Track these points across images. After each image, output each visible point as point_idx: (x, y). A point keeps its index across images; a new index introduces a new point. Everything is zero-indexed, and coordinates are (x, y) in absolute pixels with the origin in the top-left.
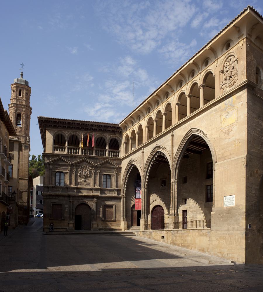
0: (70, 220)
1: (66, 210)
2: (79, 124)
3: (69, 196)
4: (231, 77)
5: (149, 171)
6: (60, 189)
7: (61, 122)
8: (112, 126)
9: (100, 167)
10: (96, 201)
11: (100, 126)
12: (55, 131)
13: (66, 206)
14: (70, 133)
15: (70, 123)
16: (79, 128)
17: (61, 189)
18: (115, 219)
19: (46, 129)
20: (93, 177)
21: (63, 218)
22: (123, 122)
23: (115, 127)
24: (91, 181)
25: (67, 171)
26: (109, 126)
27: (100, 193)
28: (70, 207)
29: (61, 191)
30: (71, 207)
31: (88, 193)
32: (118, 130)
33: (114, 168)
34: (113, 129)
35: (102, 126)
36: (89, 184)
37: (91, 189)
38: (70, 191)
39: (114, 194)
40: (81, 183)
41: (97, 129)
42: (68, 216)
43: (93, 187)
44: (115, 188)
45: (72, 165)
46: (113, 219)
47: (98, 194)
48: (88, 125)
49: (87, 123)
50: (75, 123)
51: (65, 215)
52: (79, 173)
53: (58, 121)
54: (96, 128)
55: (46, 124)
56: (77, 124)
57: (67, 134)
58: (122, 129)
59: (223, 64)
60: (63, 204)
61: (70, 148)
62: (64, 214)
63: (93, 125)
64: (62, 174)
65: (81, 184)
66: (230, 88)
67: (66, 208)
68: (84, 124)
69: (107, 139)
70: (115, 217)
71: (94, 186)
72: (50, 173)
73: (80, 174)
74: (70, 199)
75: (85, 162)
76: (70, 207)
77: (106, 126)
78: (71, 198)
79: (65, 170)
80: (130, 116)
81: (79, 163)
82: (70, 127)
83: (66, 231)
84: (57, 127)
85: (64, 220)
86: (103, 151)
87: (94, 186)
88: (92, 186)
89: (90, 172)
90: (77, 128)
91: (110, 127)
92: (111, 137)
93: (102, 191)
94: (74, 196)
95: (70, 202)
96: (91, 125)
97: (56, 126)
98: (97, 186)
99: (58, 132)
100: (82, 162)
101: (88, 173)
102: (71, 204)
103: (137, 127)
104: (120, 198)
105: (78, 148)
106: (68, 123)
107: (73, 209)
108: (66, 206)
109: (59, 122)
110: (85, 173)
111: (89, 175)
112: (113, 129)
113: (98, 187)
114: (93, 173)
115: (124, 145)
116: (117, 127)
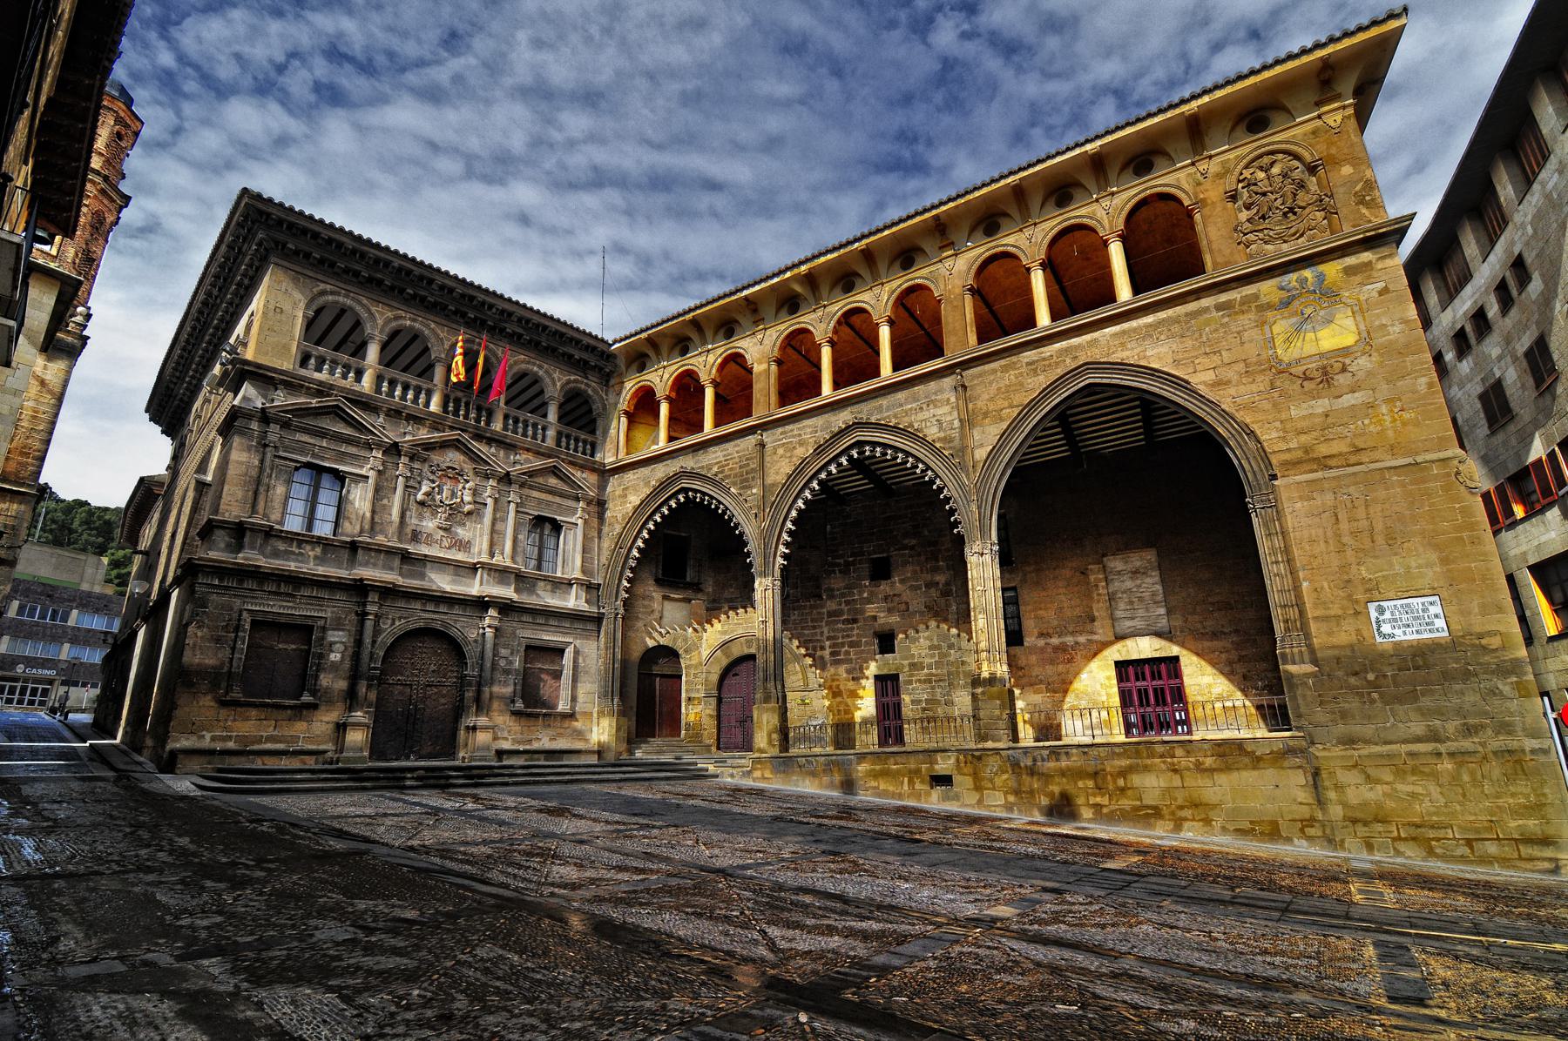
0: (351, 709)
1: (335, 657)
2: (451, 290)
3: (360, 589)
4: (1291, 210)
5: (794, 513)
6: (308, 547)
7: (363, 255)
8: (586, 340)
9: (522, 485)
10: (496, 623)
11: (538, 325)
12: (322, 286)
13: (335, 636)
14: (397, 318)
15: (409, 272)
16: (445, 308)
17: (318, 550)
18: (573, 708)
19: (273, 259)
20: (488, 519)
21: (306, 698)
22: (644, 335)
23: (594, 349)
24: (477, 536)
25: (363, 472)
26: (572, 339)
27: (516, 591)
28: (359, 642)
29: (316, 557)
30: (367, 640)
31: (453, 582)
32: (601, 363)
33: (577, 499)
34: (585, 356)
35: (545, 328)
36: (465, 546)
37: (474, 568)
38: (366, 564)
39: (574, 601)
40: (429, 535)
41: (520, 336)
42: (342, 685)
43: (485, 558)
44: (577, 574)
45: (393, 450)
46: (562, 706)
47: (508, 592)
48: (491, 306)
49: (489, 300)
50: (431, 281)
51: (325, 680)
52: (425, 489)
53: (350, 244)
54: (520, 330)
55: (281, 237)
56: (442, 287)
57: (379, 319)
58: (621, 362)
59: (1236, 173)
60: (321, 623)
61: (387, 376)
62: (317, 677)
63: (510, 314)
64: (326, 481)
65: (430, 540)
66: (1285, 247)
67: (332, 644)
68: (472, 298)
69: (554, 384)
70: (574, 699)
71: (492, 555)
72: (262, 461)
73: (427, 494)
74: (364, 605)
75: (458, 449)
76: (359, 642)
77: (562, 335)
78: (373, 597)
79: (345, 464)
80: (687, 317)
81: (429, 447)
82: (402, 291)
83: (319, 767)
84: (335, 273)
85: (314, 707)
86: (535, 426)
87: (492, 555)
88: (480, 553)
89: (475, 492)
90: (435, 305)
91: (578, 342)
92: (569, 382)
93: (520, 579)
94: (389, 593)
95: (365, 614)
96: (503, 311)
97: (332, 265)
98: (503, 559)
99: (339, 294)
100: (444, 445)
101: (467, 498)
102: (369, 624)
103: (666, 376)
104: (598, 620)
105: (425, 386)
106: (400, 269)
107: (372, 654)
108: (335, 636)
109: (354, 252)
110: (453, 495)
111: (467, 508)
112: (585, 356)
113: (508, 563)
114: (489, 501)
115: (624, 420)
116: (603, 352)
